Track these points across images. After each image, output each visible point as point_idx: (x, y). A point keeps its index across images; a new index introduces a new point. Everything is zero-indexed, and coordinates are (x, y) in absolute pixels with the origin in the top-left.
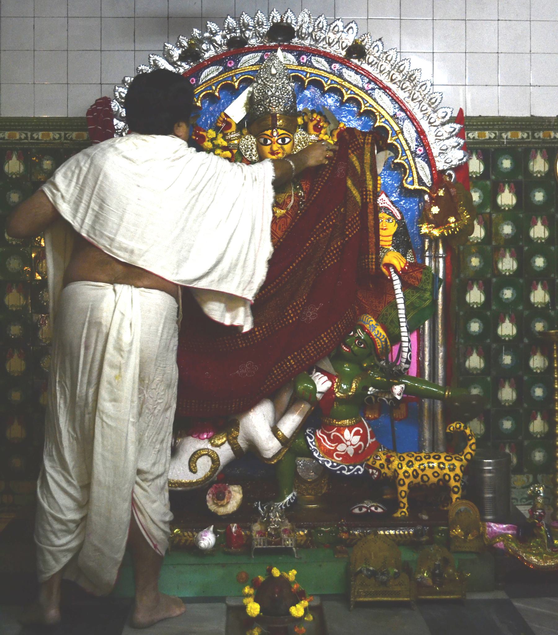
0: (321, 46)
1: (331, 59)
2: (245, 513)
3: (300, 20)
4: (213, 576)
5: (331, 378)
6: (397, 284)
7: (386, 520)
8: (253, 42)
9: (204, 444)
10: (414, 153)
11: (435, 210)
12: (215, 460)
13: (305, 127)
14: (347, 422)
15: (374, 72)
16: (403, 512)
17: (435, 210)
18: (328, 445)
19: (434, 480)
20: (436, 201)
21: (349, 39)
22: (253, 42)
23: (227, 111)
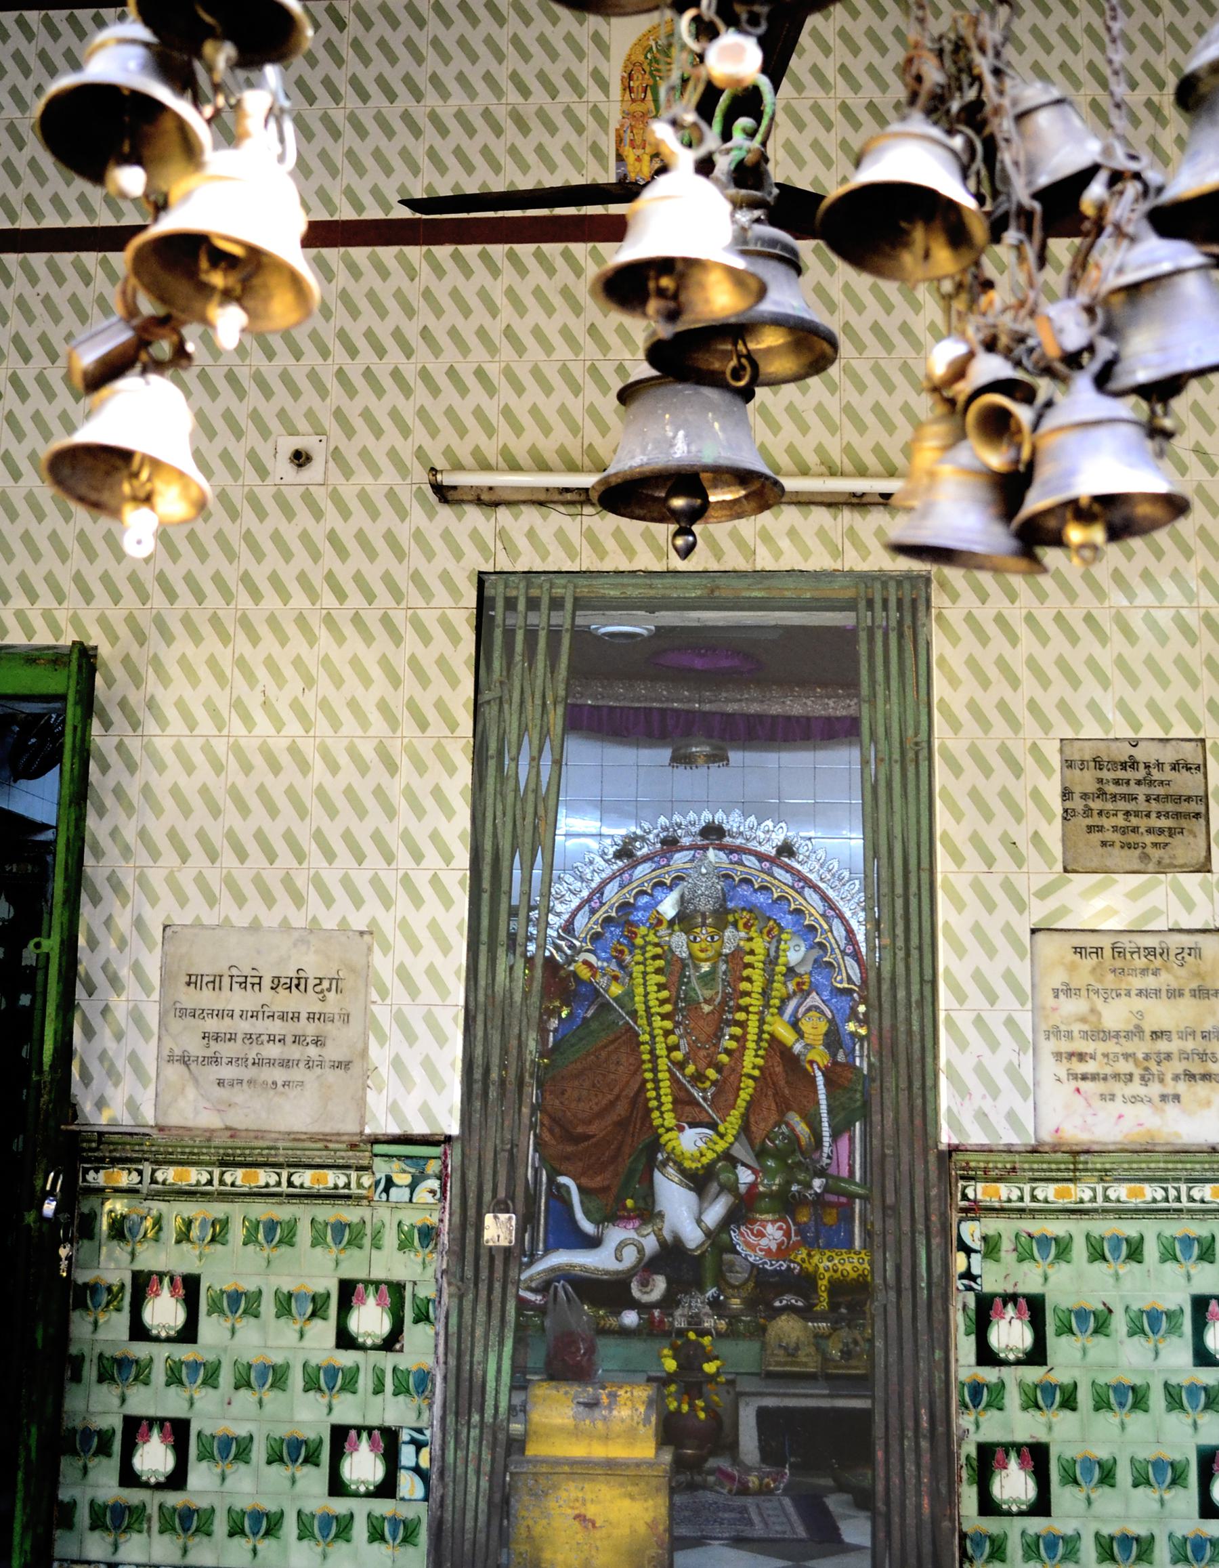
0: (750, 845)
1: (761, 857)
2: (669, 1302)
3: (733, 822)
4: (637, 1347)
5: (755, 1172)
6: (820, 1080)
7: (806, 1313)
8: (686, 841)
9: (632, 1234)
10: (843, 952)
11: (862, 1009)
12: (641, 1250)
13: (735, 924)
14: (769, 1217)
15: (804, 869)
16: (823, 1304)
17: (862, 1009)
18: (752, 1239)
19: (853, 1275)
20: (864, 1000)
21: (778, 838)
22: (686, 841)
23: (661, 908)
